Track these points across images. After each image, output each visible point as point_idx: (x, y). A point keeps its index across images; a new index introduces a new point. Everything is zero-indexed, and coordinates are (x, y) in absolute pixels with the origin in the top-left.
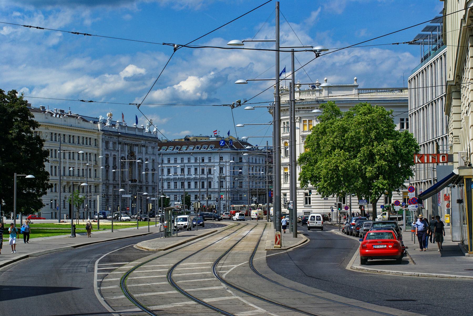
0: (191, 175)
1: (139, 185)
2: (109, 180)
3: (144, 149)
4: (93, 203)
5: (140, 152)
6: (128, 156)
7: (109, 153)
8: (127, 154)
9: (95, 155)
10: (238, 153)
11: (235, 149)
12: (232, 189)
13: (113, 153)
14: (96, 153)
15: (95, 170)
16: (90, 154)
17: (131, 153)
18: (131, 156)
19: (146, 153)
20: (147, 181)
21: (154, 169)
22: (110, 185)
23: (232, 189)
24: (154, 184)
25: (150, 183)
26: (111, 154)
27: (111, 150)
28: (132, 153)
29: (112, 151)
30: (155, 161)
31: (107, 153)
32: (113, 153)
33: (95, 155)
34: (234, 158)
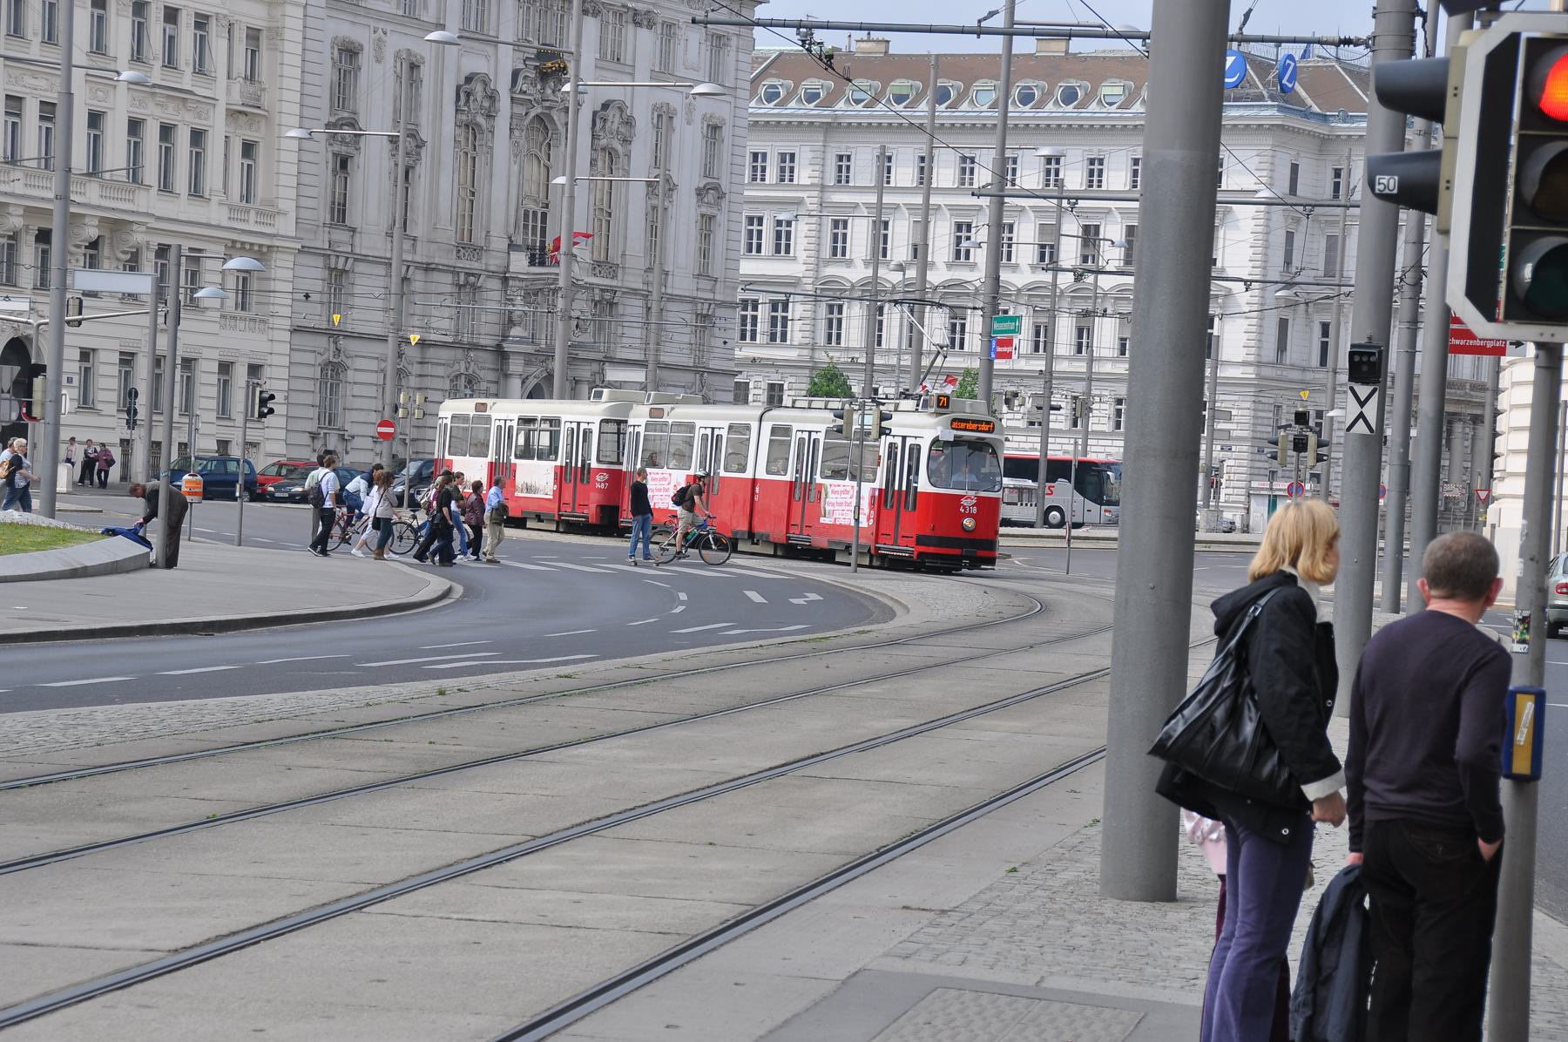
0: (849, 263)
1: (590, 287)
2: (353, 230)
3: (643, 43)
4: (214, 379)
5: (613, 58)
6: (515, 74)
7: (361, 35)
8: (508, 60)
9: (254, 35)
10: (1325, 143)
11: (1307, 114)
12: (1267, 372)
13: (396, 42)
14: (256, 24)
15: (248, 149)
16: (201, 22)
17: (542, 55)
18: (544, 76)
19: (664, 69)
20: (656, 265)
21: (717, 188)
22: (360, 267)
23: (1267, 372)
24: (713, 291)
25: (682, 283)
26: (379, 45)
27: (379, 16)
28: (555, 56)
29: (389, 27)
30: (726, 132)
31: (345, 29)
32: (396, 42)
33: (254, 35)
34: (1295, 168)
